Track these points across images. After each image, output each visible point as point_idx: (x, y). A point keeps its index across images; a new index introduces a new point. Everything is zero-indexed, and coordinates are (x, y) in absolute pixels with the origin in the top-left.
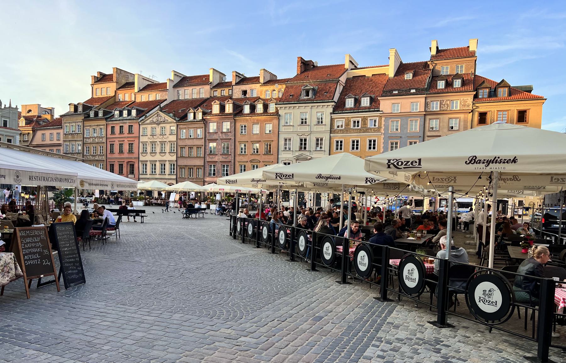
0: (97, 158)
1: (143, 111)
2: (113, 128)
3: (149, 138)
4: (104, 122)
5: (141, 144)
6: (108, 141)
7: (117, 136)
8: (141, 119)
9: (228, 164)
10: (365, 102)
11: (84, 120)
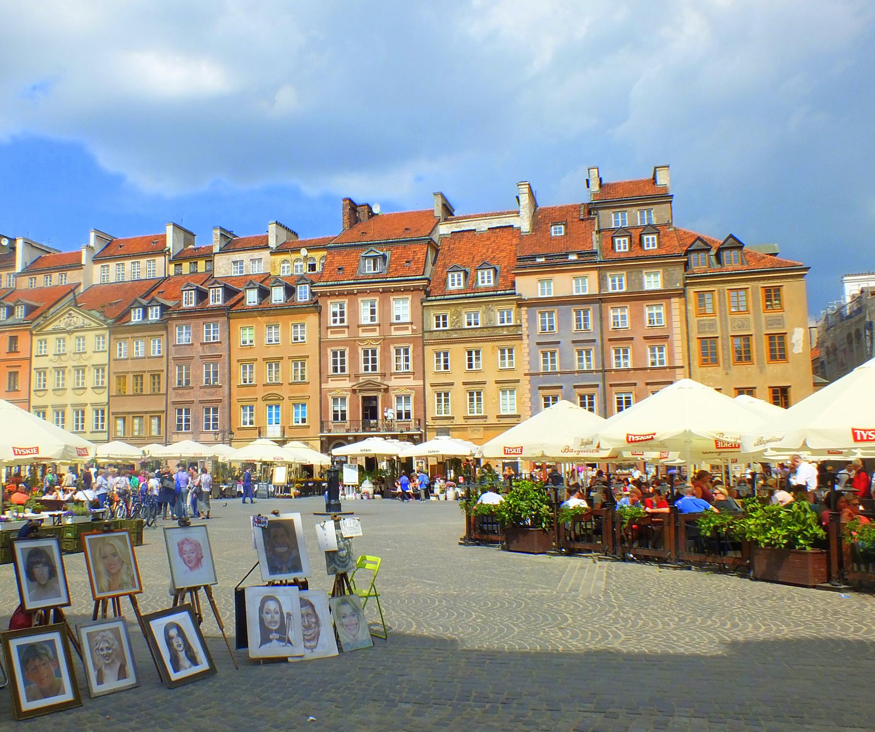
1: (37, 307)
5: (34, 372)
8: (35, 323)
10: (485, 279)
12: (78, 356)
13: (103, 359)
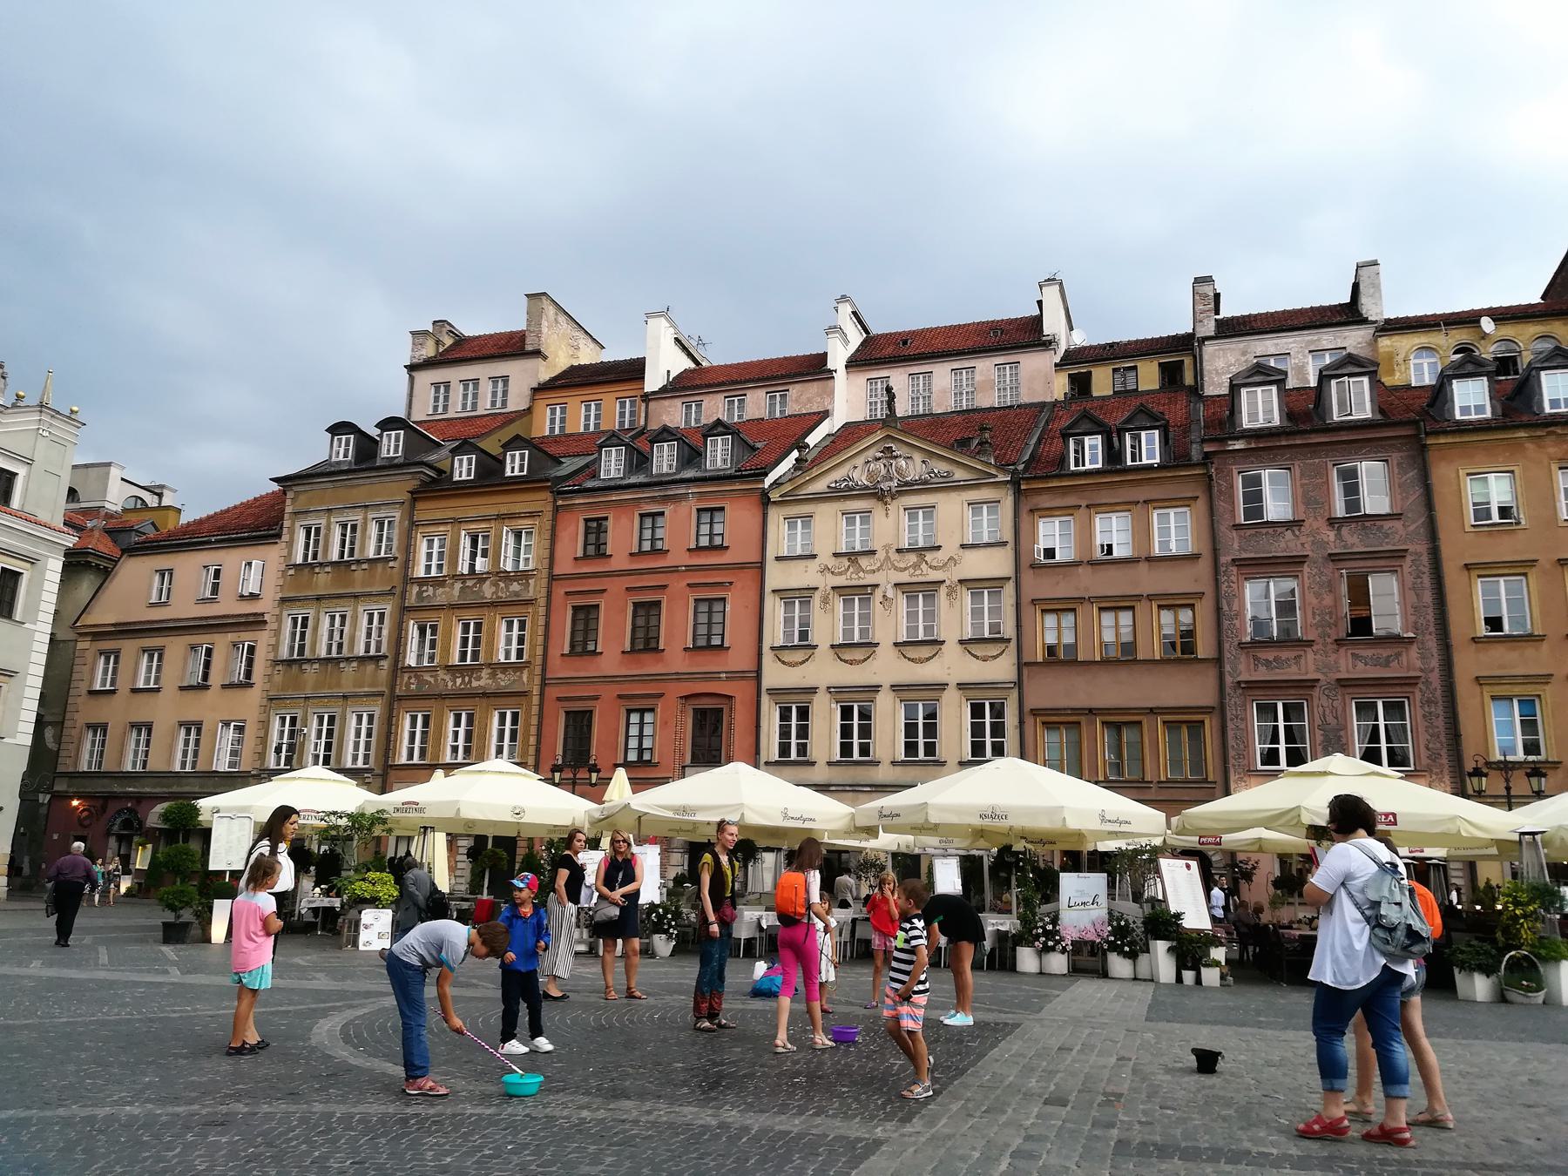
0: (483, 681)
2: (596, 530)
3: (825, 569)
4: (540, 501)
7: (619, 562)
11: (417, 496)
12: (913, 558)
13: (997, 564)
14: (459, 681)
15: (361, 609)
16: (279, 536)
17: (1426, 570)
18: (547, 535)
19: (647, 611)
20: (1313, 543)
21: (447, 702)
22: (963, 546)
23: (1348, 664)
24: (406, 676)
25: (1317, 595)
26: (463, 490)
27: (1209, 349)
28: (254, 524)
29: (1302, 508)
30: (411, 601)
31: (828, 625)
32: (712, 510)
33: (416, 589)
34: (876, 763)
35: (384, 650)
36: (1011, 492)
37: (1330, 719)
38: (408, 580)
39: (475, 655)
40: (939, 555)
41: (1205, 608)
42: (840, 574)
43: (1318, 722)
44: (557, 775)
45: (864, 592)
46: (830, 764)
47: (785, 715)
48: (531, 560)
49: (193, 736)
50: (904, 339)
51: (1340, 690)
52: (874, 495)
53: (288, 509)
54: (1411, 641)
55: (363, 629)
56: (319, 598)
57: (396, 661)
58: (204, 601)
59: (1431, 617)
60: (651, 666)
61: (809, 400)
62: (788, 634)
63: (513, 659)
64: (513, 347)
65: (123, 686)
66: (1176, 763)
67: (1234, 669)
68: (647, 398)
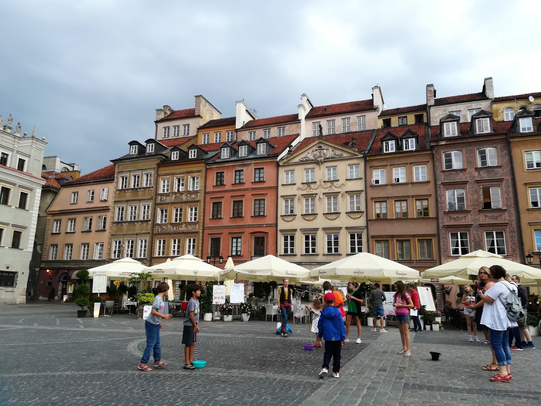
0: (183, 228)
2: (220, 176)
3: (299, 189)
4: (201, 167)
6: (208, 197)
7: (228, 187)
9: (500, 229)
11: (159, 166)
12: (329, 184)
13: (359, 186)
14: (175, 228)
15: (141, 204)
16: (113, 180)
17: (511, 185)
18: (204, 178)
19: (238, 204)
20: (470, 177)
21: (171, 236)
22: (347, 180)
23: (483, 219)
24: (157, 227)
25: (472, 195)
26: (175, 163)
27: (432, 110)
28: (105, 177)
29: (466, 164)
30: (159, 202)
31: (300, 208)
32: (260, 169)
33: (160, 197)
34: (318, 255)
35: (149, 218)
36: (363, 161)
37: (477, 238)
38: (157, 194)
39: (180, 219)
40: (339, 183)
41: (432, 200)
42: (304, 190)
43: (472, 239)
44: (209, 260)
45: (313, 196)
46: (301, 255)
47: (286, 239)
48: (198, 186)
49: (86, 248)
50: (325, 108)
51: (480, 228)
52: (315, 163)
53: (116, 171)
54: (505, 210)
55: (142, 211)
56: (127, 201)
57: (154, 222)
58: (89, 202)
59: (512, 202)
60: (240, 223)
61: (292, 130)
62: (286, 211)
63: (193, 221)
64: (191, 114)
65: (63, 231)
66: (422, 254)
67: (443, 221)
68: (237, 131)
